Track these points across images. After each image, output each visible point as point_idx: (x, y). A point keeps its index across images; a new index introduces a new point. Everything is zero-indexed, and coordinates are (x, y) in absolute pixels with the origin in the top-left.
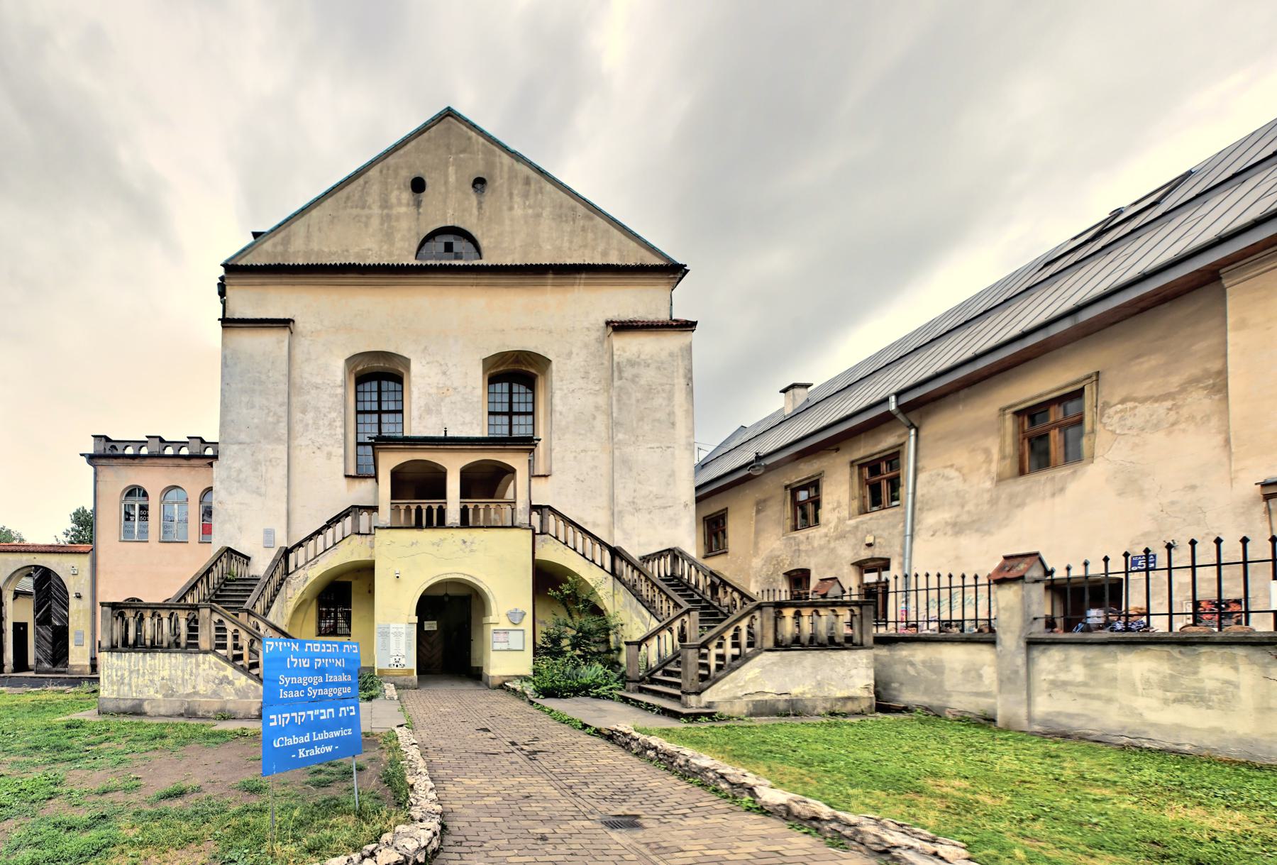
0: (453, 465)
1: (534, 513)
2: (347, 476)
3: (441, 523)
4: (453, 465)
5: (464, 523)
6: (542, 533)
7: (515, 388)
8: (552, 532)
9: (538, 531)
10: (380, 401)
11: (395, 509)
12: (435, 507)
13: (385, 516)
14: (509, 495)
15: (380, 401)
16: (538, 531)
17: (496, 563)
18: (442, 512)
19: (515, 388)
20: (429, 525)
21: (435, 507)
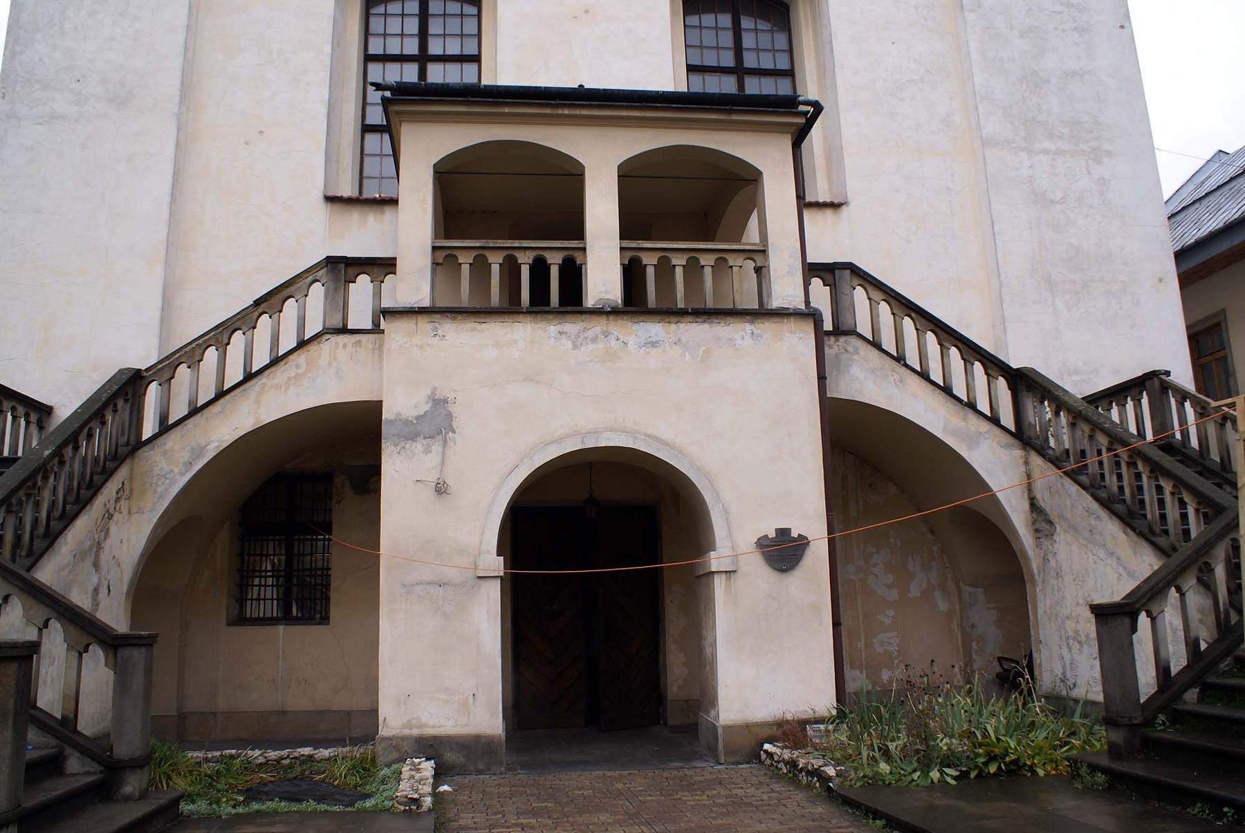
0: (602, 160)
1: (816, 283)
2: (331, 199)
3: (574, 298)
4: (602, 160)
5: (634, 302)
6: (838, 332)
7: (746, 23)
8: (864, 329)
9: (828, 326)
10: (423, 35)
11: (443, 261)
12: (555, 261)
13: (413, 284)
14: (752, 235)
15: (423, 35)
16: (828, 326)
17: (732, 420)
18: (573, 275)
19: (746, 23)
20: (540, 305)
21: (555, 261)
